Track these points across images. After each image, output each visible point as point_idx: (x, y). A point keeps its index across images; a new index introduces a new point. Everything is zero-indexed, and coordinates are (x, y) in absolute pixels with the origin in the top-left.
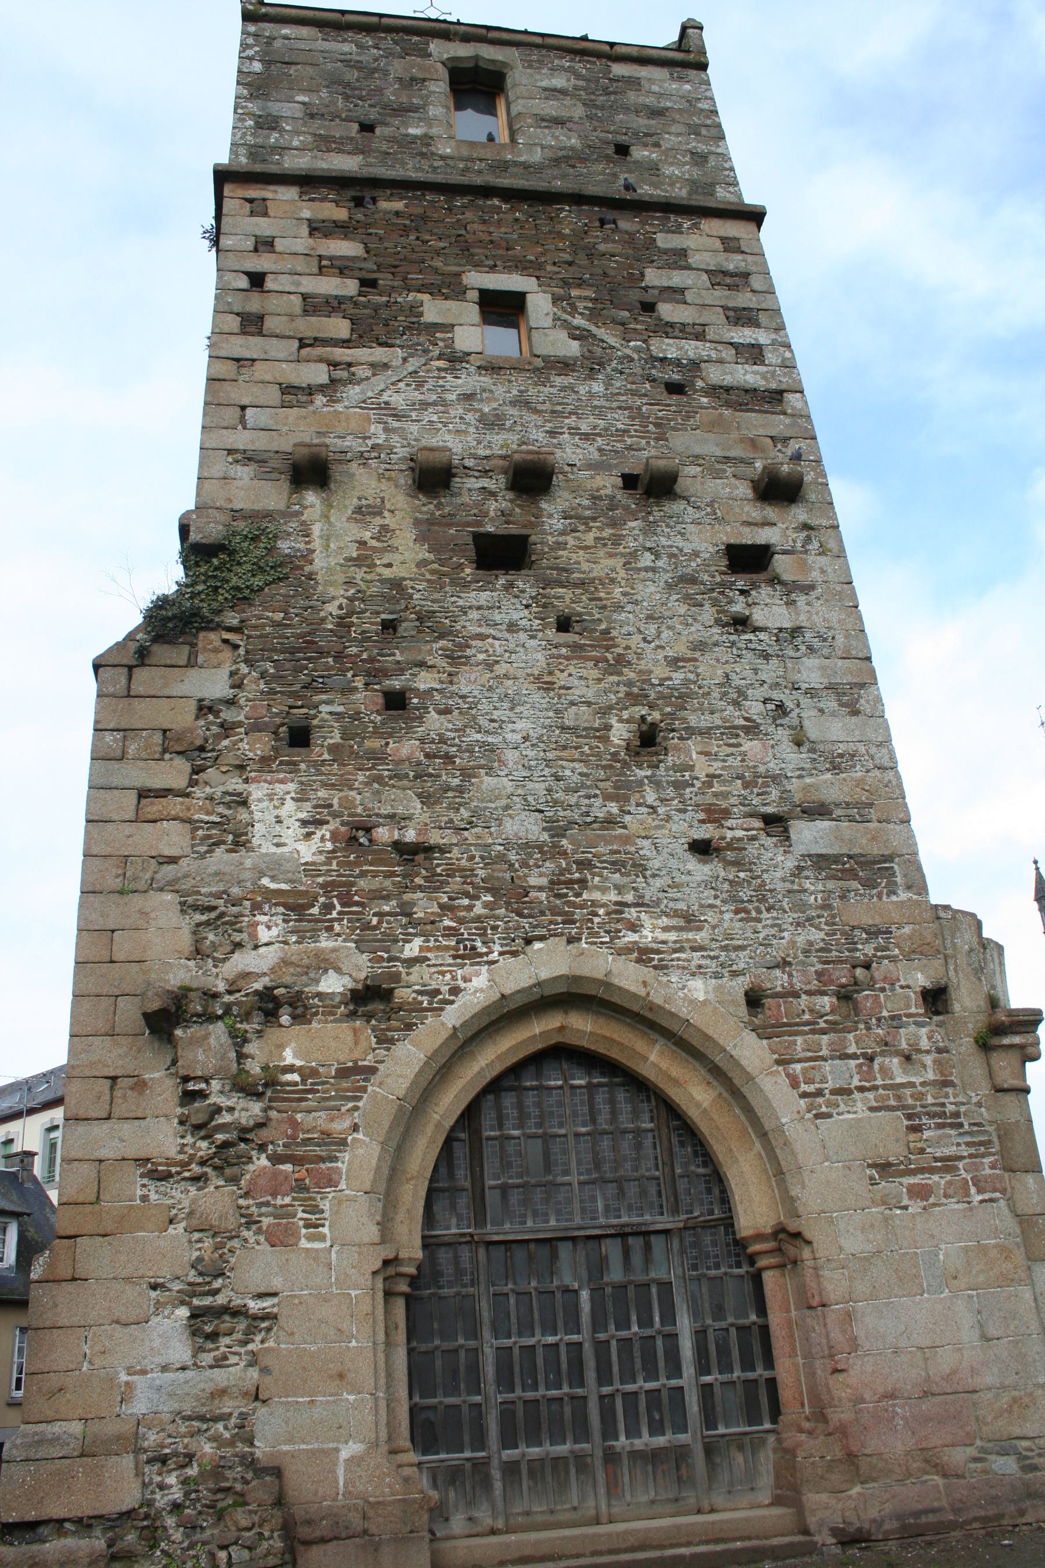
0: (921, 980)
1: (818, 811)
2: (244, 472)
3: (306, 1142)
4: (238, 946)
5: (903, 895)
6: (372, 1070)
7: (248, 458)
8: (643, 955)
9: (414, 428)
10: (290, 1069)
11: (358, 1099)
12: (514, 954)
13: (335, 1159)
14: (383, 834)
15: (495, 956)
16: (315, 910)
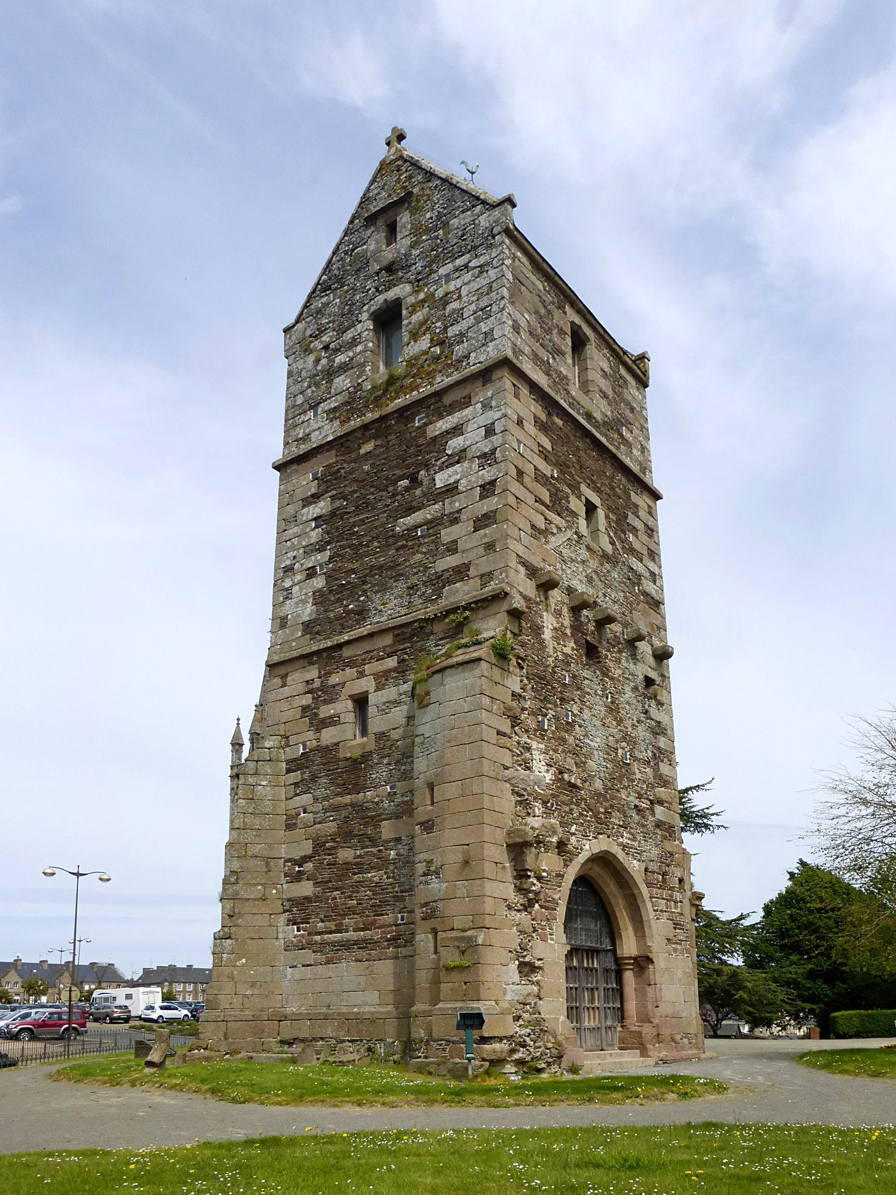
0: (679, 874)
1: (660, 802)
2: (522, 570)
3: (549, 901)
4: (529, 814)
5: (677, 842)
6: (562, 876)
7: (524, 564)
8: (624, 847)
9: (569, 571)
10: (544, 871)
11: (560, 887)
12: (595, 838)
13: (555, 910)
14: (566, 776)
15: (590, 838)
16: (549, 805)
